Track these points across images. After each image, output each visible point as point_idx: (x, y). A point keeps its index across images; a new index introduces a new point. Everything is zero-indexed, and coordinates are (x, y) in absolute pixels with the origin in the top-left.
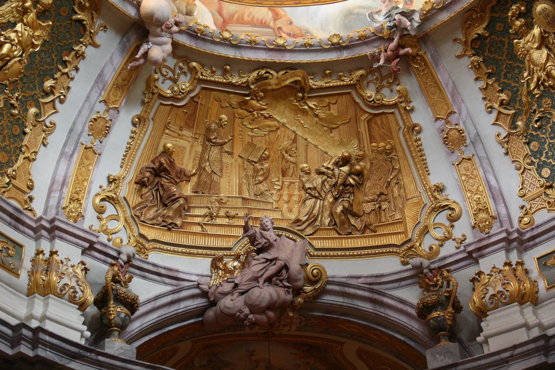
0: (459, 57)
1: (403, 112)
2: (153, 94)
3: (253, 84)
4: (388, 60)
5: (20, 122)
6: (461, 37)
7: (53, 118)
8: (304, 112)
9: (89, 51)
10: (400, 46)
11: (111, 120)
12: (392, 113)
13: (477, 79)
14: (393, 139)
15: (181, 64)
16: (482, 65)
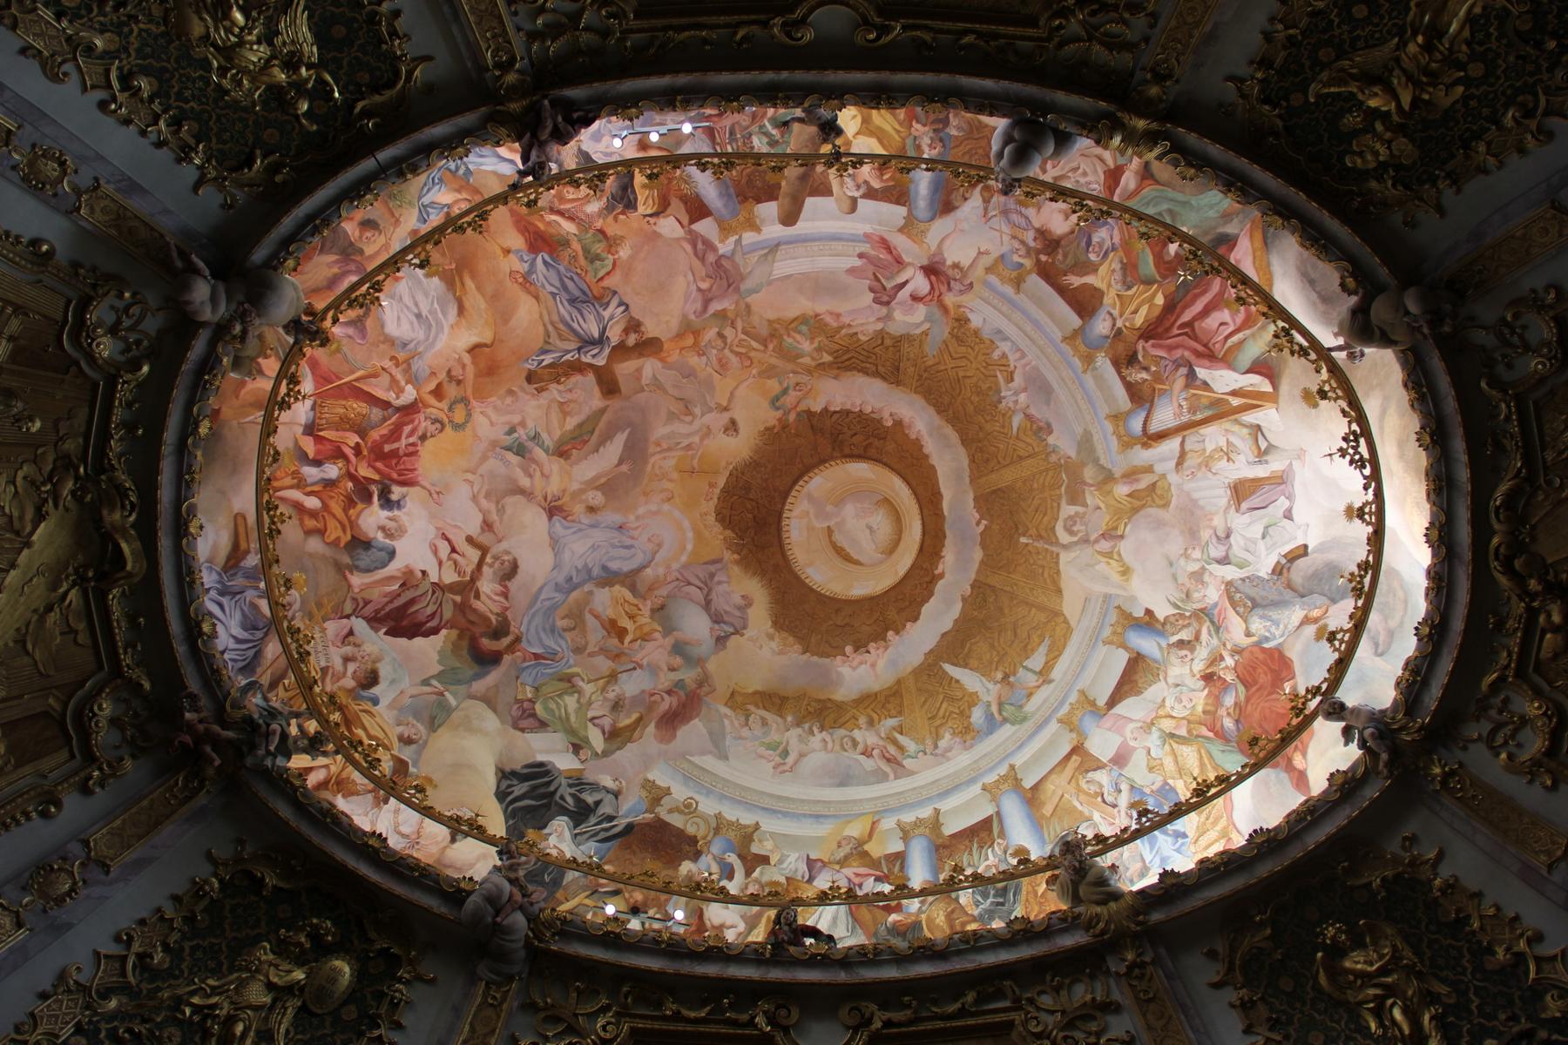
0: (209, 856)
1: (82, 774)
2: (94, 286)
3: (110, 480)
4: (190, 727)
5: (83, 12)
6: (249, 849)
7: (74, 81)
8: (54, 587)
9: (189, 173)
10: (217, 743)
11: (55, 195)
12: (72, 756)
13: (176, 899)
14: (16, 767)
15: (145, 343)
16: (205, 902)
